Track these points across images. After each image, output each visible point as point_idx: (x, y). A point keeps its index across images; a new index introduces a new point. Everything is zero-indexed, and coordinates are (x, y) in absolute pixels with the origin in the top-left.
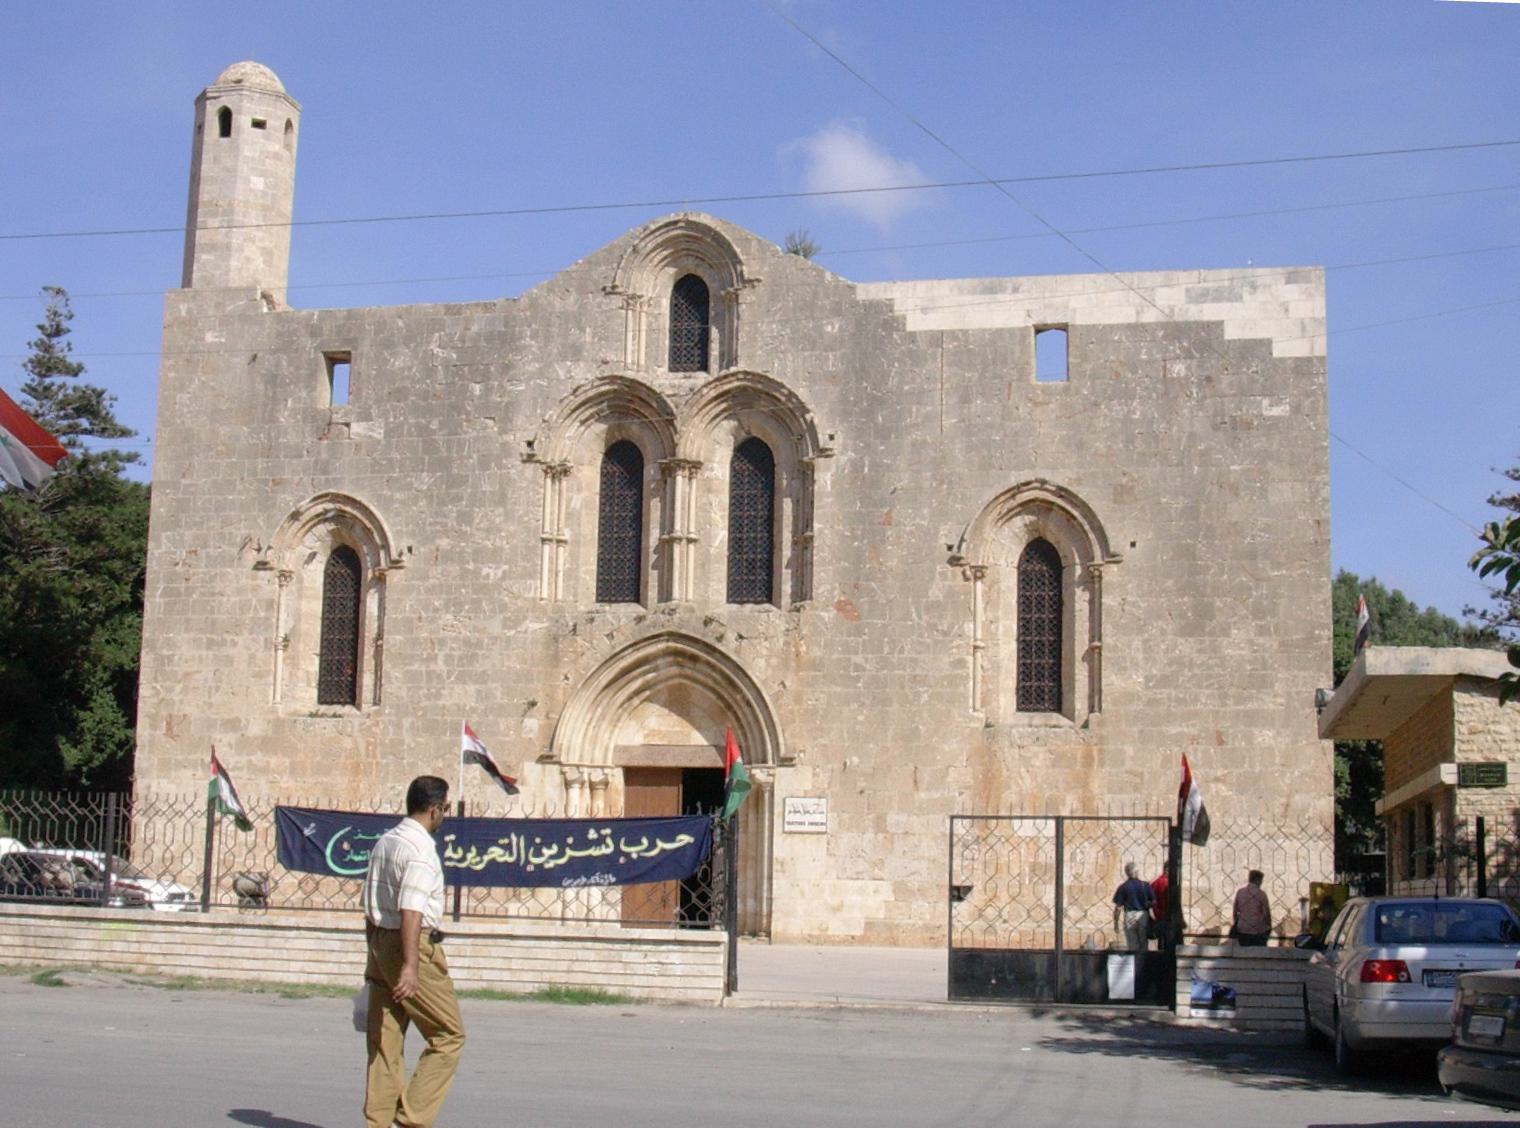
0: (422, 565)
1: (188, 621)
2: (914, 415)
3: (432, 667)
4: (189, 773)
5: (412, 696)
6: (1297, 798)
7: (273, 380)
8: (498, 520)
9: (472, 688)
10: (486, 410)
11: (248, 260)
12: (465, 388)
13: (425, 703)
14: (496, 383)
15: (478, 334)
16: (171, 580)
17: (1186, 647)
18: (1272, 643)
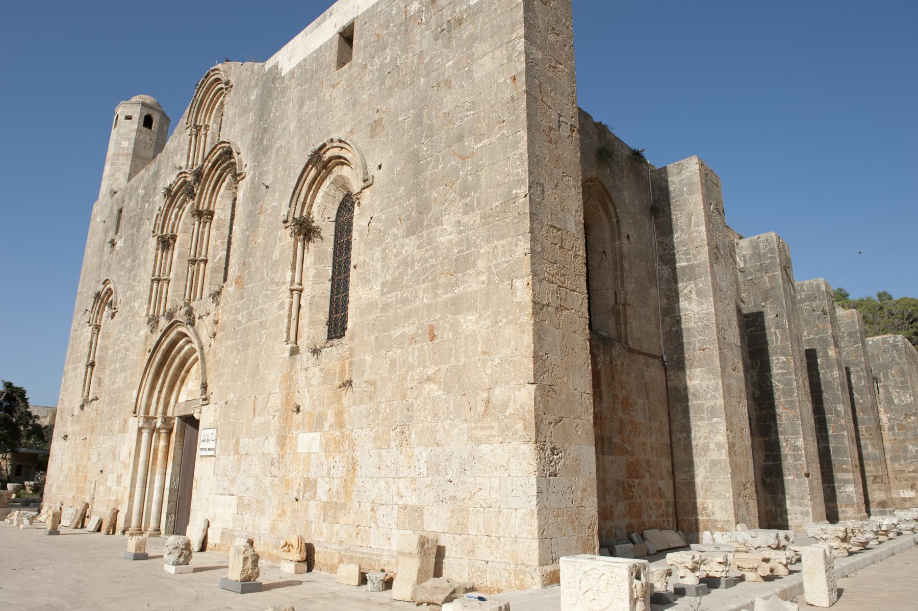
6: (497, 391)
11: (116, 179)
17: (410, 245)
18: (475, 218)
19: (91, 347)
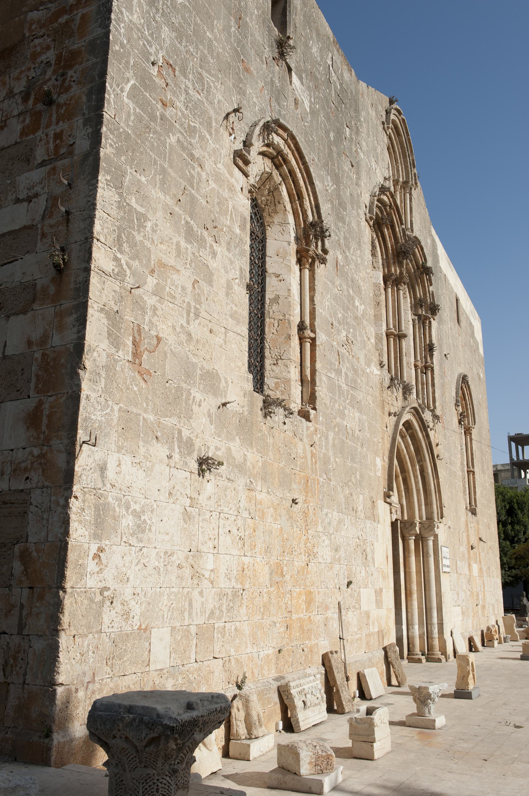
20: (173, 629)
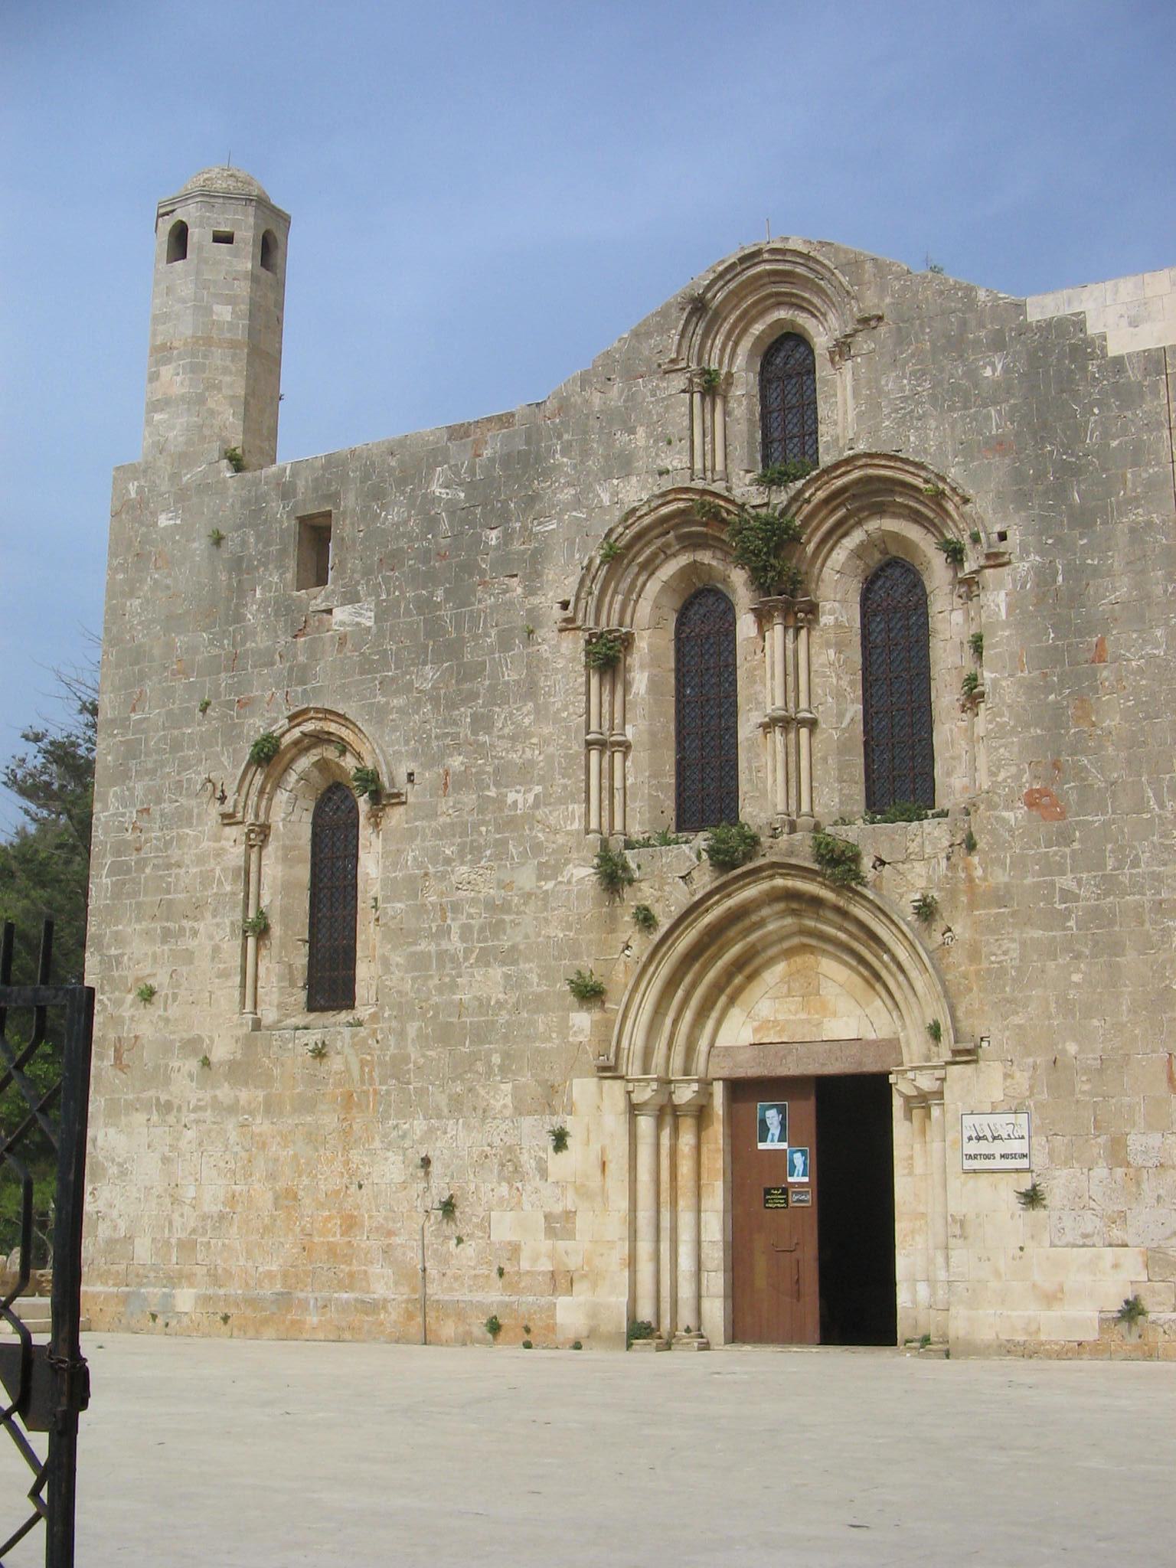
0: (428, 799)
1: (139, 905)
2: (1129, 485)
3: (445, 945)
4: (140, 1118)
5: (418, 990)
7: (237, 564)
8: (527, 721)
9: (497, 972)
10: (507, 565)
11: (212, 413)
12: (477, 540)
13: (436, 999)
14: (518, 525)
15: (492, 460)
16: (118, 853)
19: (247, 883)
20: (153, 1239)
